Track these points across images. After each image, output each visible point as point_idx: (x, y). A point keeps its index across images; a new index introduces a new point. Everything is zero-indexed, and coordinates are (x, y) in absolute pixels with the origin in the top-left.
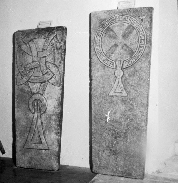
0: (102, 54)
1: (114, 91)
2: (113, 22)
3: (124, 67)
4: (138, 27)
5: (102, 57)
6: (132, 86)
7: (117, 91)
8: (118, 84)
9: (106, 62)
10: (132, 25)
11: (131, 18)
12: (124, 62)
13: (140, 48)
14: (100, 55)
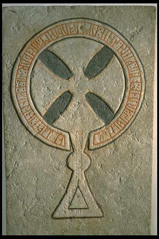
0: (34, 114)
1: (67, 204)
2: (61, 35)
3: (92, 146)
4: (124, 52)
6: (111, 191)
7: (75, 205)
8: (78, 187)
9: (45, 135)
10: (110, 46)
11: (106, 31)
12: (92, 134)
13: (129, 102)
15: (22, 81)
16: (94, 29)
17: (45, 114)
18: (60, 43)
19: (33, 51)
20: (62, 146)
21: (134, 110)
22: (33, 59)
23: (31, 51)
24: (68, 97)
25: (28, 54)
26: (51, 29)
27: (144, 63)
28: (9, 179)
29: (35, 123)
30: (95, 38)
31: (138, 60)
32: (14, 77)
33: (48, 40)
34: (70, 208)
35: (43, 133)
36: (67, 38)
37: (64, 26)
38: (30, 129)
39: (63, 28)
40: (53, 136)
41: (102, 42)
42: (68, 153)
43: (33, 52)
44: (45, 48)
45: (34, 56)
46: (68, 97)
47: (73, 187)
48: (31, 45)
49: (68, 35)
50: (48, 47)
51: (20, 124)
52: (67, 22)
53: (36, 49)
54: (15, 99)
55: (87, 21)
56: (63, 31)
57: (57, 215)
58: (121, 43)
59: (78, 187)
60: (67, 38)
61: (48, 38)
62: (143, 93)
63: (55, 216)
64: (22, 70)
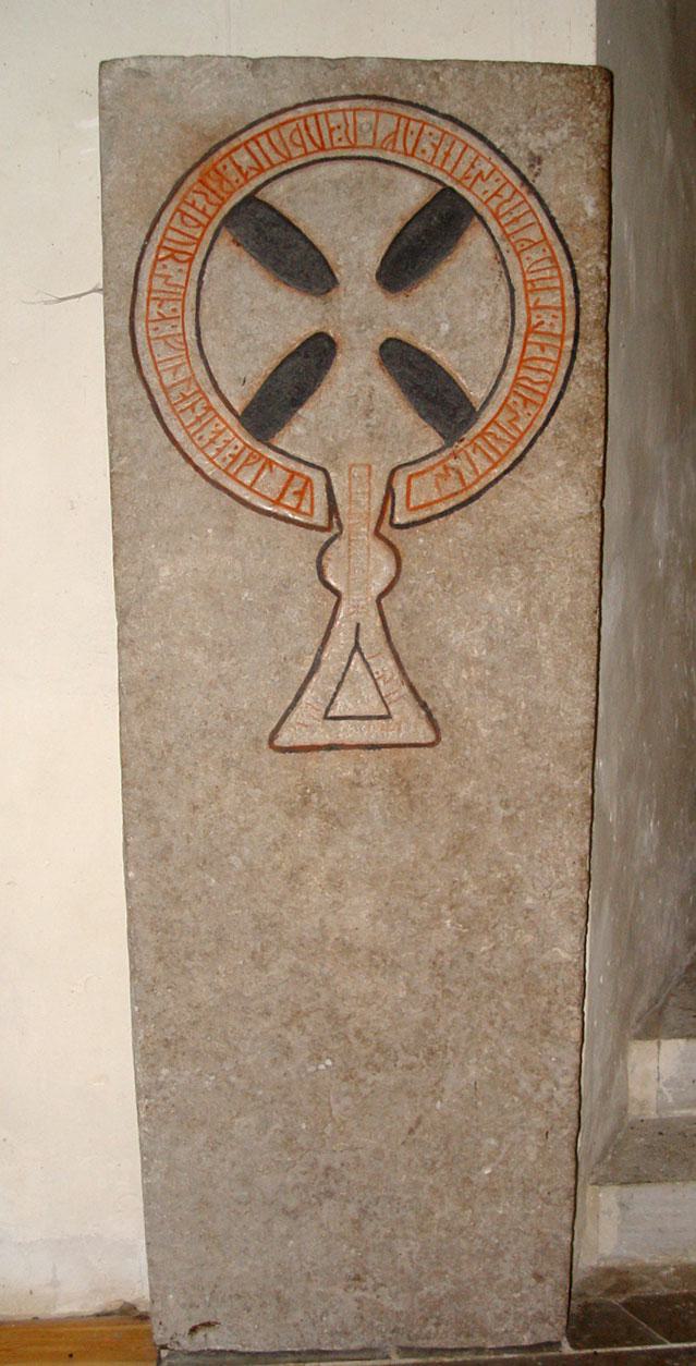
0: (209, 408)
2: (297, 152)
4: (506, 207)
5: (208, 435)
6: (467, 662)
8: (357, 647)
13: (523, 373)
14: (189, 419)
15: (168, 300)
16: (409, 133)
17: (247, 411)
18: (297, 177)
19: (208, 201)
20: (305, 514)
21: (539, 399)
22: (206, 227)
23: (200, 201)
24: (316, 355)
25: (191, 212)
26: (266, 132)
27: (573, 247)
28: (128, 621)
29: (212, 436)
30: (415, 164)
31: (552, 236)
32: (143, 284)
33: (256, 166)
34: (329, 715)
35: (398, 125)
36: (322, 160)
37: (311, 121)
38: (199, 459)
39: (307, 128)
40: (272, 483)
41: (438, 175)
42: (326, 536)
43: (208, 206)
44: (248, 190)
45: (211, 219)
46: (316, 355)
47: (342, 639)
48: (201, 181)
49: (322, 148)
50: (258, 189)
51: (167, 442)
52: (319, 108)
53: (219, 196)
54: (145, 359)
55: (386, 106)
56: (306, 139)
57: (284, 739)
58: (497, 180)
59: (357, 647)
60: (322, 160)
61: (256, 159)
62: (569, 343)
63: (279, 742)
64: (169, 263)
